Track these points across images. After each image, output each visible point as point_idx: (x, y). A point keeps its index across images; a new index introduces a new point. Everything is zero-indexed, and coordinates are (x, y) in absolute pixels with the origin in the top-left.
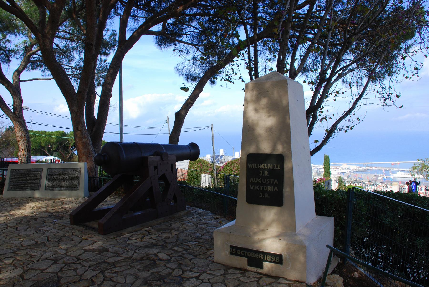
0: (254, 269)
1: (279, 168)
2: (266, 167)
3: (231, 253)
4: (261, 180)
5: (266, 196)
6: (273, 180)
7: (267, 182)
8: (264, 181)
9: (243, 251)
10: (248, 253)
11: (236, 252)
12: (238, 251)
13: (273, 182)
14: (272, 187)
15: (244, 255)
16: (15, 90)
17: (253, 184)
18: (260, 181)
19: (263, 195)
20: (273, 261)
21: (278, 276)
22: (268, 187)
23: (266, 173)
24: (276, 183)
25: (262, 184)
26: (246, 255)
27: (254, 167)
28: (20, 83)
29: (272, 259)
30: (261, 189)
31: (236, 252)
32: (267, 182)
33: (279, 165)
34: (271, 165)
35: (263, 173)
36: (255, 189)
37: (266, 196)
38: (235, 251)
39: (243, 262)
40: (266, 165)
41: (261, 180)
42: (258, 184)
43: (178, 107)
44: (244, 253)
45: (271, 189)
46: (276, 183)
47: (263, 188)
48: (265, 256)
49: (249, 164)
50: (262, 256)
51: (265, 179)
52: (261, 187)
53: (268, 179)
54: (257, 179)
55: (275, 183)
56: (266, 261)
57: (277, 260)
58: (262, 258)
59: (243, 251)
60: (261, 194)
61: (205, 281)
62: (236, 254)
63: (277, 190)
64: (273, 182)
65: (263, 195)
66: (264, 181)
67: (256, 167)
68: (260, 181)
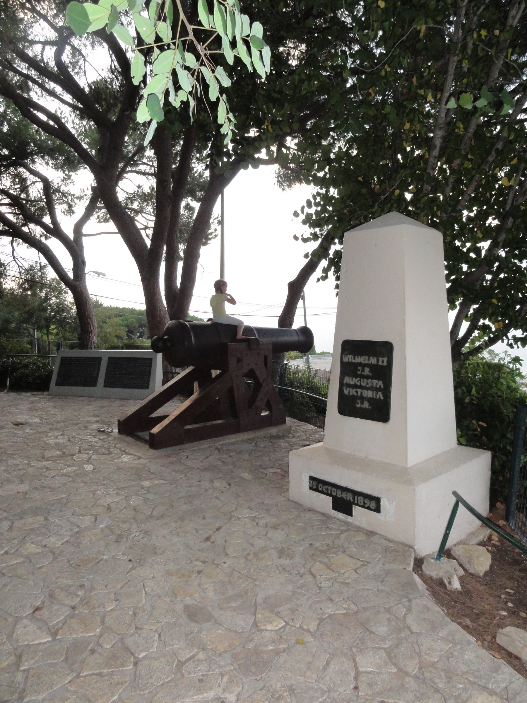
0: (341, 516)
1: (385, 364)
2: (367, 362)
3: (311, 488)
4: (360, 380)
5: (366, 405)
10: (333, 489)
11: (317, 486)
12: (320, 485)
13: (377, 384)
16: (75, 248)
17: (349, 386)
18: (358, 382)
19: (362, 403)
20: (366, 506)
21: (374, 530)
23: (367, 371)
24: (380, 386)
25: (361, 387)
26: (329, 492)
28: (84, 238)
29: (365, 503)
30: (359, 395)
31: (317, 486)
32: (368, 384)
33: (385, 359)
35: (363, 371)
37: (366, 405)
38: (318, 485)
39: (325, 502)
42: (355, 386)
43: (293, 276)
44: (327, 489)
46: (380, 386)
47: (362, 393)
48: (356, 497)
49: (343, 356)
52: (359, 391)
55: (378, 386)
56: (357, 505)
57: (373, 505)
58: (352, 500)
59: (326, 487)
60: (359, 401)
61: (260, 524)
62: (317, 490)
63: (382, 398)
64: (377, 384)
67: (353, 361)
68: (358, 382)
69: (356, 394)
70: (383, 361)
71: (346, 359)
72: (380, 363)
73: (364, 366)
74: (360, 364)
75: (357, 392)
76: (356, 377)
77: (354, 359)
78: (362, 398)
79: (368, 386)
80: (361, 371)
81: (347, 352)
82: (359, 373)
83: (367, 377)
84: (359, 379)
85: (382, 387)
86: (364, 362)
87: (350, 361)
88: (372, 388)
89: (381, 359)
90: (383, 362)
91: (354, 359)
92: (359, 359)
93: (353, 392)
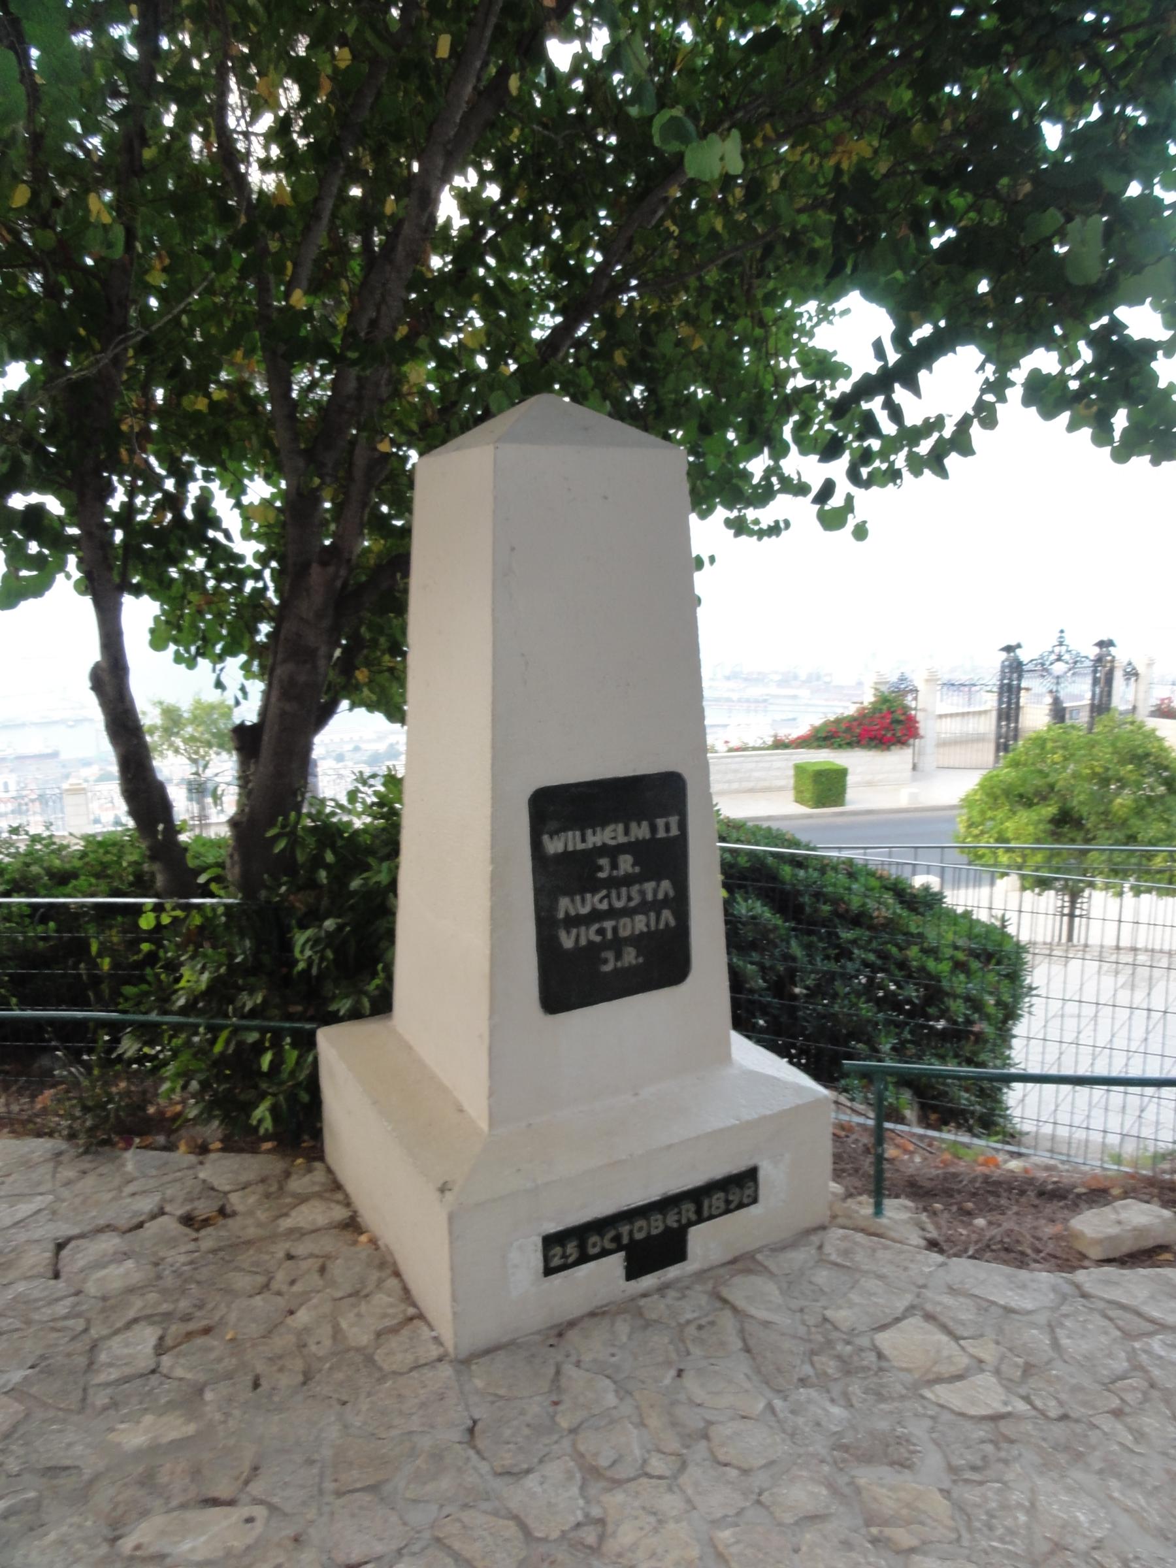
1: (674, 831)
2: (622, 839)
4: (608, 896)
5: (630, 957)
7: (630, 899)
8: (619, 898)
9: (611, 1234)
17: (574, 921)
18: (601, 901)
23: (626, 864)
25: (612, 913)
30: (609, 935)
33: (674, 820)
34: (645, 824)
35: (614, 866)
37: (630, 957)
41: (608, 896)
42: (596, 916)
45: (648, 925)
52: (608, 925)
55: (661, 896)
60: (610, 955)
64: (655, 892)
65: (618, 957)
66: (619, 898)
67: (581, 846)
68: (601, 901)
69: (598, 939)
70: (666, 827)
71: (554, 846)
72: (661, 834)
73: (612, 852)
74: (604, 850)
75: (601, 932)
76: (594, 891)
77: (583, 840)
78: (617, 944)
79: (632, 904)
80: (607, 868)
81: (553, 825)
82: (602, 875)
83: (628, 881)
84: (604, 892)
85: (671, 893)
86: (613, 843)
87: (570, 848)
88: (644, 907)
89: (660, 822)
90: (667, 829)
91: (583, 840)
92: (595, 838)
93: (590, 934)
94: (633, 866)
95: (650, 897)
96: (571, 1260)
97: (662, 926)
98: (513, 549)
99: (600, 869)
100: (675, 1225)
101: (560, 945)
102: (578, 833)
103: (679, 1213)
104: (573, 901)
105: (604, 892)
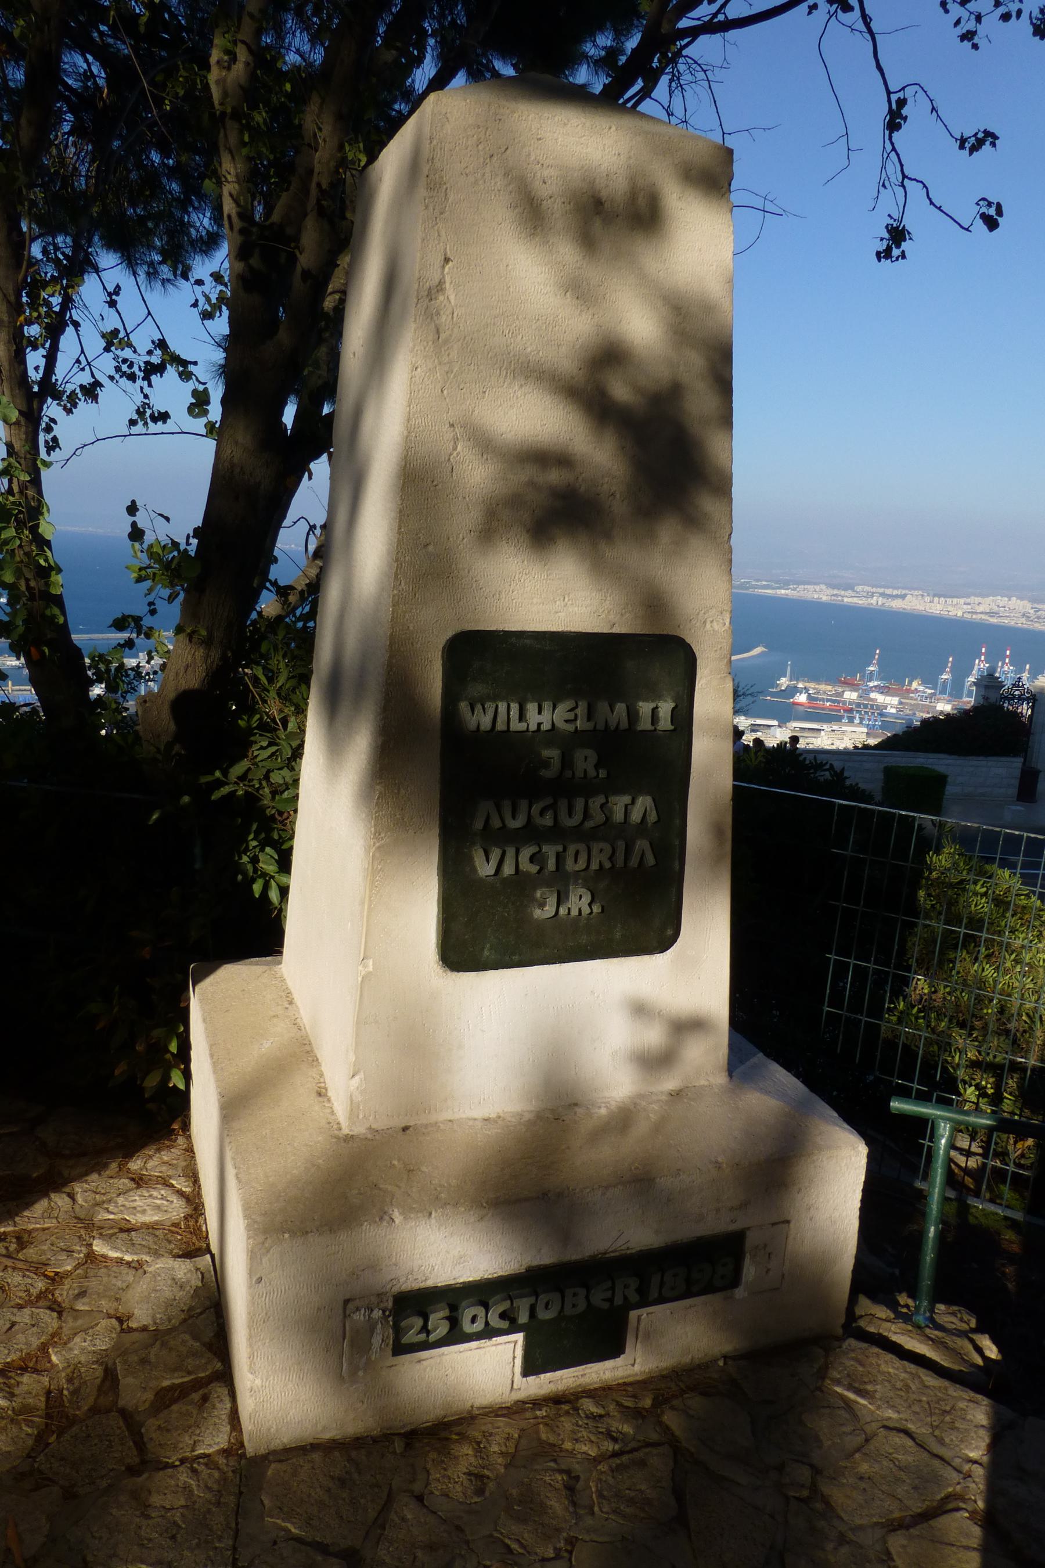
4: (553, 807)
6: (626, 799)
7: (586, 815)
14: (621, 845)
15: (513, 1321)
22: (596, 847)
27: (500, 726)
32: (586, 815)
36: (508, 870)
40: (583, 706)
47: (560, 858)
49: (464, 706)
50: (633, 1283)
51: (579, 804)
52: (550, 851)
53: (601, 799)
54: (524, 804)
55: (636, 816)
63: (650, 860)
67: (516, 726)
68: (542, 814)
72: (645, 724)
77: (522, 717)
79: (589, 824)
81: (477, 689)
84: (549, 801)
85: (653, 817)
86: (570, 728)
87: (500, 726)
91: (522, 717)
94: (597, 767)
95: (619, 816)
96: (433, 1338)
97: (634, 862)
98: (447, 260)
99: (546, 764)
100: (606, 1306)
101: (474, 870)
102: (515, 707)
103: (613, 1288)
104: (499, 808)
105: (549, 801)
